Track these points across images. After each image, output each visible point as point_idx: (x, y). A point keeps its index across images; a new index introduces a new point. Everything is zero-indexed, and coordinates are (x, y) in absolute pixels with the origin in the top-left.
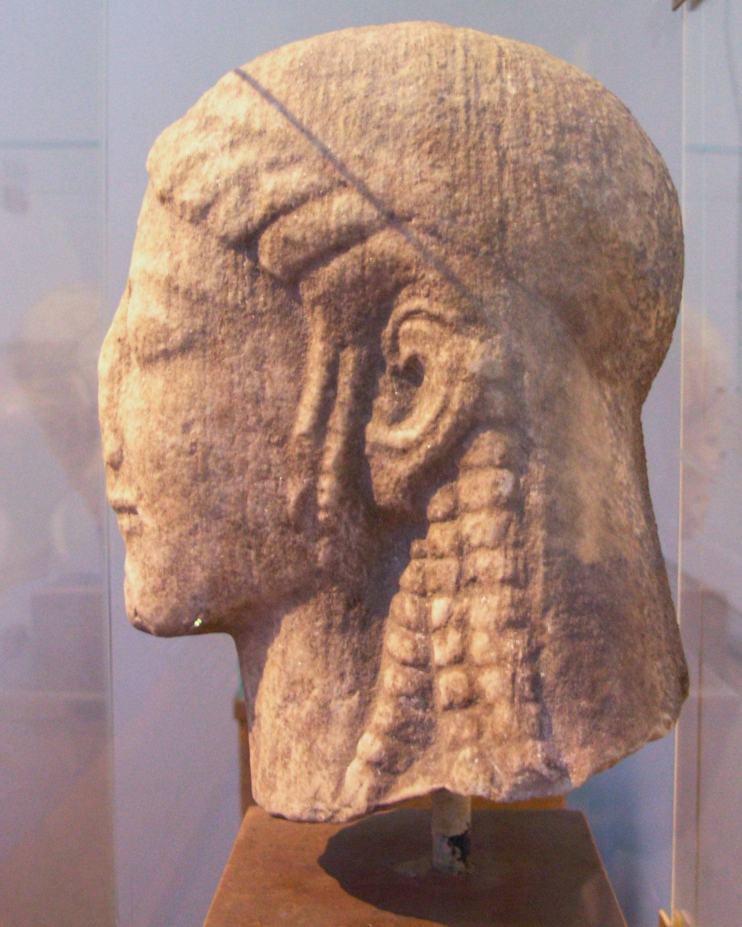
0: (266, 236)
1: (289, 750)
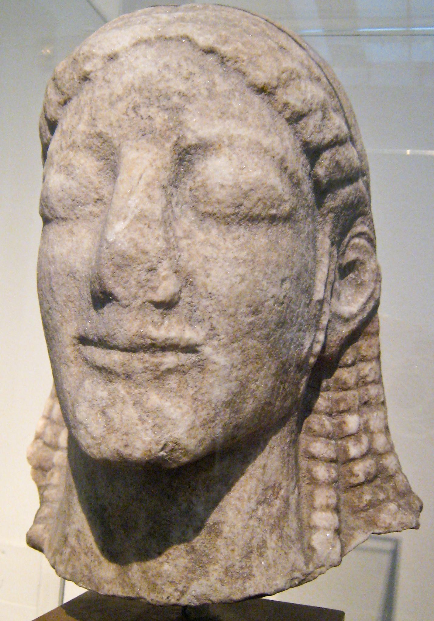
0: (327, 155)
1: (264, 541)
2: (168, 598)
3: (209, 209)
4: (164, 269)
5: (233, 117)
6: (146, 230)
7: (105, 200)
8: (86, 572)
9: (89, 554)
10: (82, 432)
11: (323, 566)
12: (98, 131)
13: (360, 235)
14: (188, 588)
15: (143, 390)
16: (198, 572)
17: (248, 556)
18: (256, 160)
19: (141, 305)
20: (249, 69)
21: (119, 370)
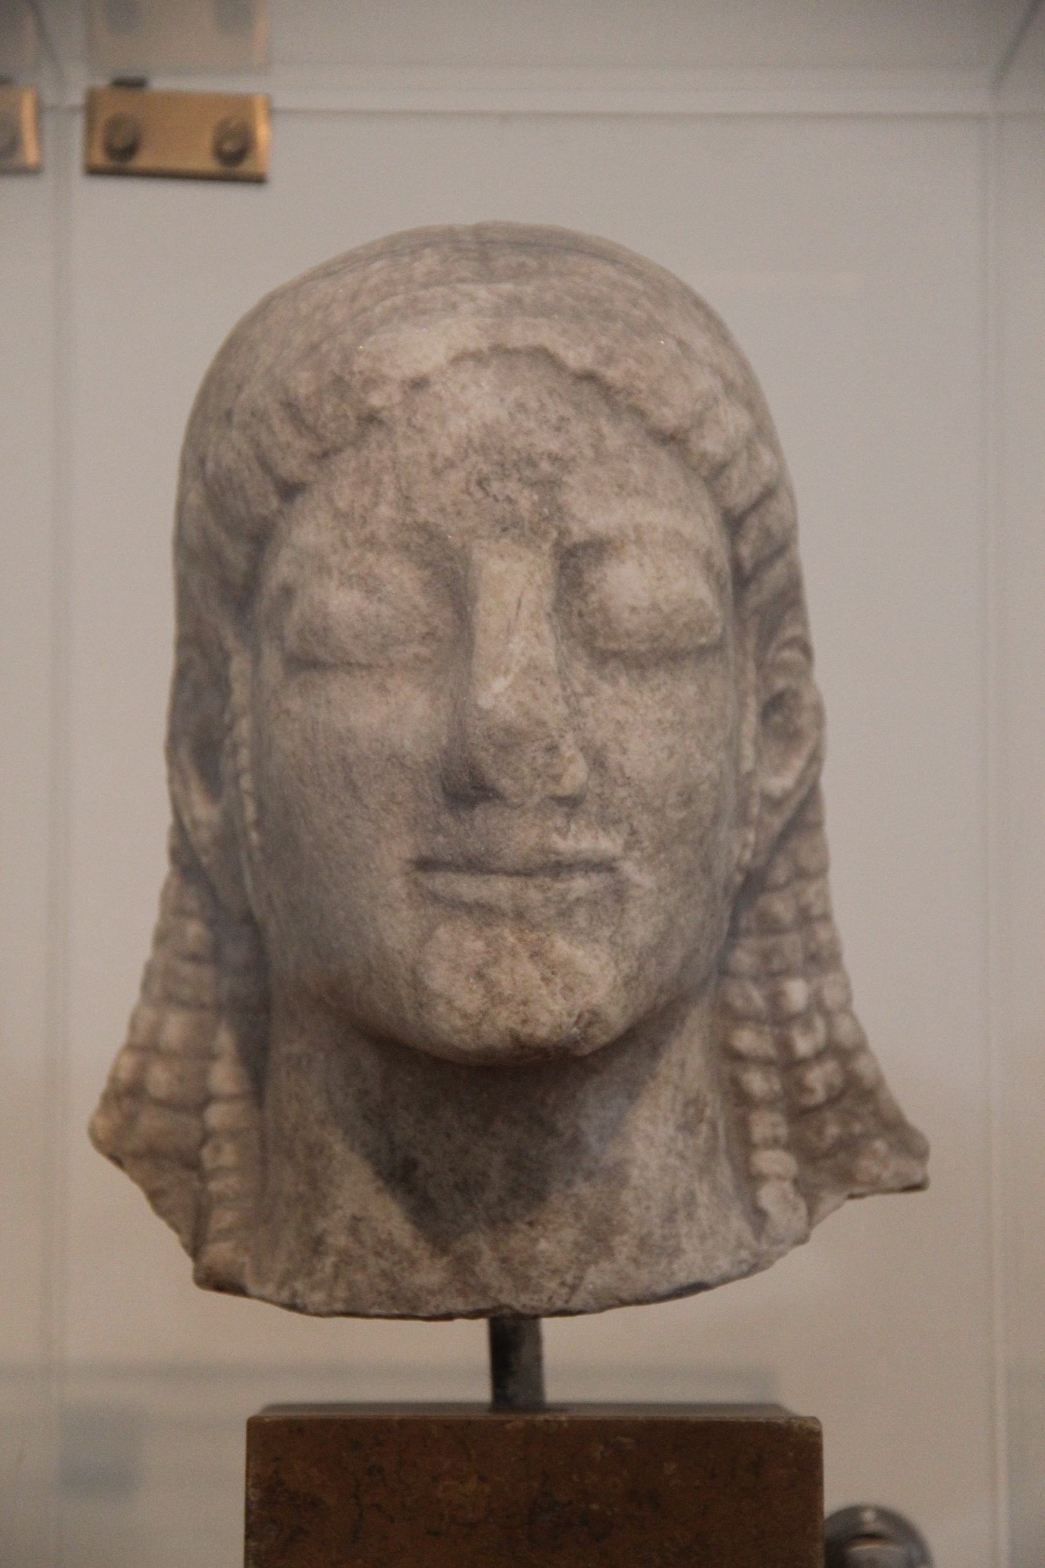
0: (753, 521)
1: (692, 1194)
2: (550, 1298)
3: (613, 646)
4: (569, 748)
5: (637, 491)
6: (539, 689)
7: (440, 633)
8: (383, 1286)
9: (387, 1253)
10: (442, 1009)
11: (782, 1241)
12: (420, 519)
13: (790, 643)
14: (581, 1278)
15: (543, 935)
16: (595, 1250)
17: (670, 1218)
18: (677, 562)
19: (539, 804)
20: (650, 406)
21: (506, 905)
